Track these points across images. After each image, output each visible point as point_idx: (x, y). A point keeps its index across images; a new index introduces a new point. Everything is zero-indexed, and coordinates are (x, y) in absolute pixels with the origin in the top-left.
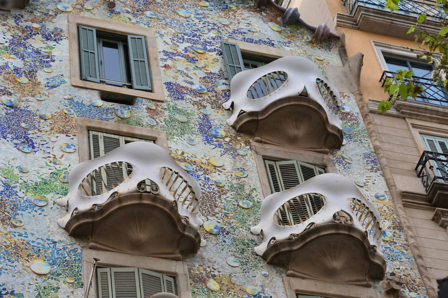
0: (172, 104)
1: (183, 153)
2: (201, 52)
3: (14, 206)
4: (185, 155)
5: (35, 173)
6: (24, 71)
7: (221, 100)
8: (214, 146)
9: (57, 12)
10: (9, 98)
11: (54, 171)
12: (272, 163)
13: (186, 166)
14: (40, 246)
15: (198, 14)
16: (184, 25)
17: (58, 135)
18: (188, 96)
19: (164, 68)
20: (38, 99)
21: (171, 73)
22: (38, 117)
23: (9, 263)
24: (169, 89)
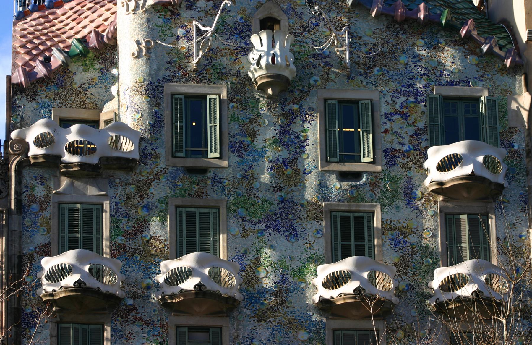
0: (387, 172)
1: (391, 222)
2: (413, 105)
3: (287, 290)
4: (392, 224)
5: (298, 259)
6: (289, 162)
7: (422, 158)
8: (413, 209)
9: (311, 87)
10: (280, 194)
11: (310, 255)
12: (451, 217)
13: (392, 235)
14: (302, 319)
15: (415, 57)
16: (403, 73)
17: (312, 221)
18: (399, 160)
19: (384, 134)
20: (299, 187)
21: (389, 137)
22: (299, 206)
23: (287, 336)
24: (386, 156)
